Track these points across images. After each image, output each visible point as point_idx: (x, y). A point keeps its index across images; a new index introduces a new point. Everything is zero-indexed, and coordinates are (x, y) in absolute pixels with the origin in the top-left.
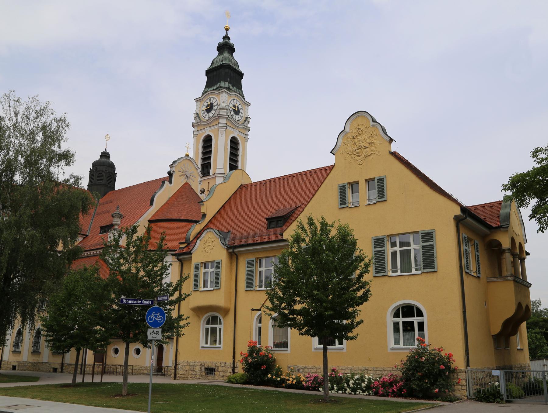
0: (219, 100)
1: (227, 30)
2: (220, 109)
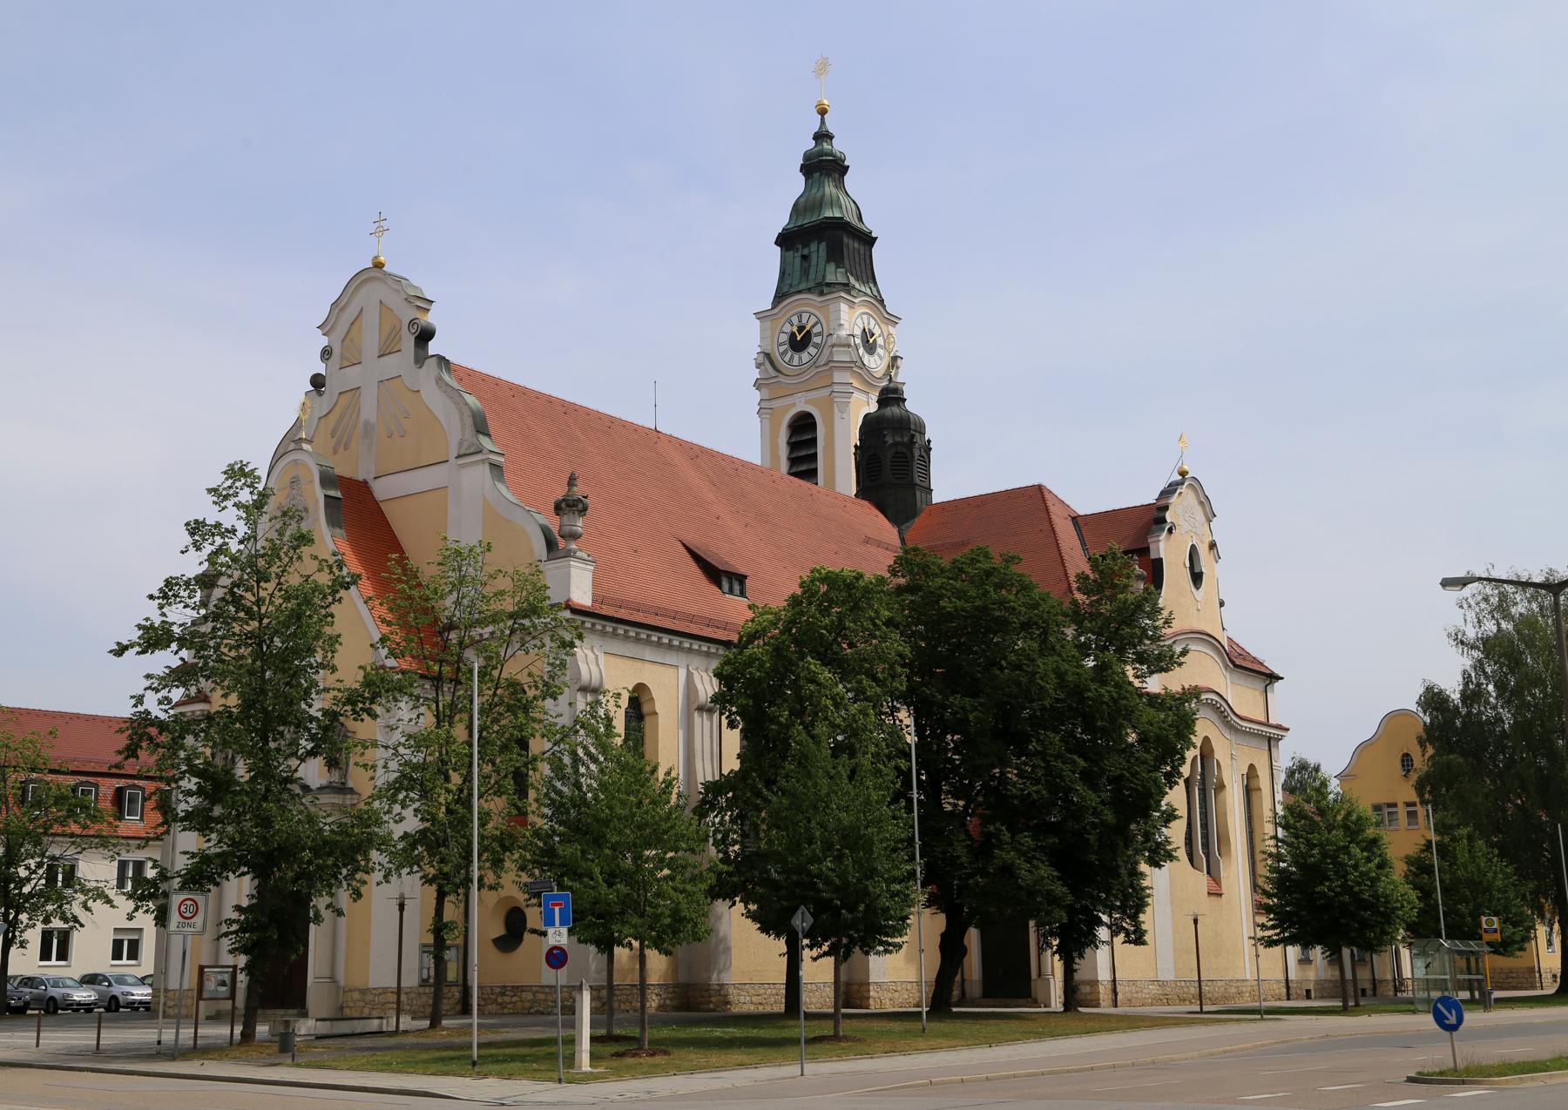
0: (828, 322)
1: (823, 112)
2: (833, 346)
